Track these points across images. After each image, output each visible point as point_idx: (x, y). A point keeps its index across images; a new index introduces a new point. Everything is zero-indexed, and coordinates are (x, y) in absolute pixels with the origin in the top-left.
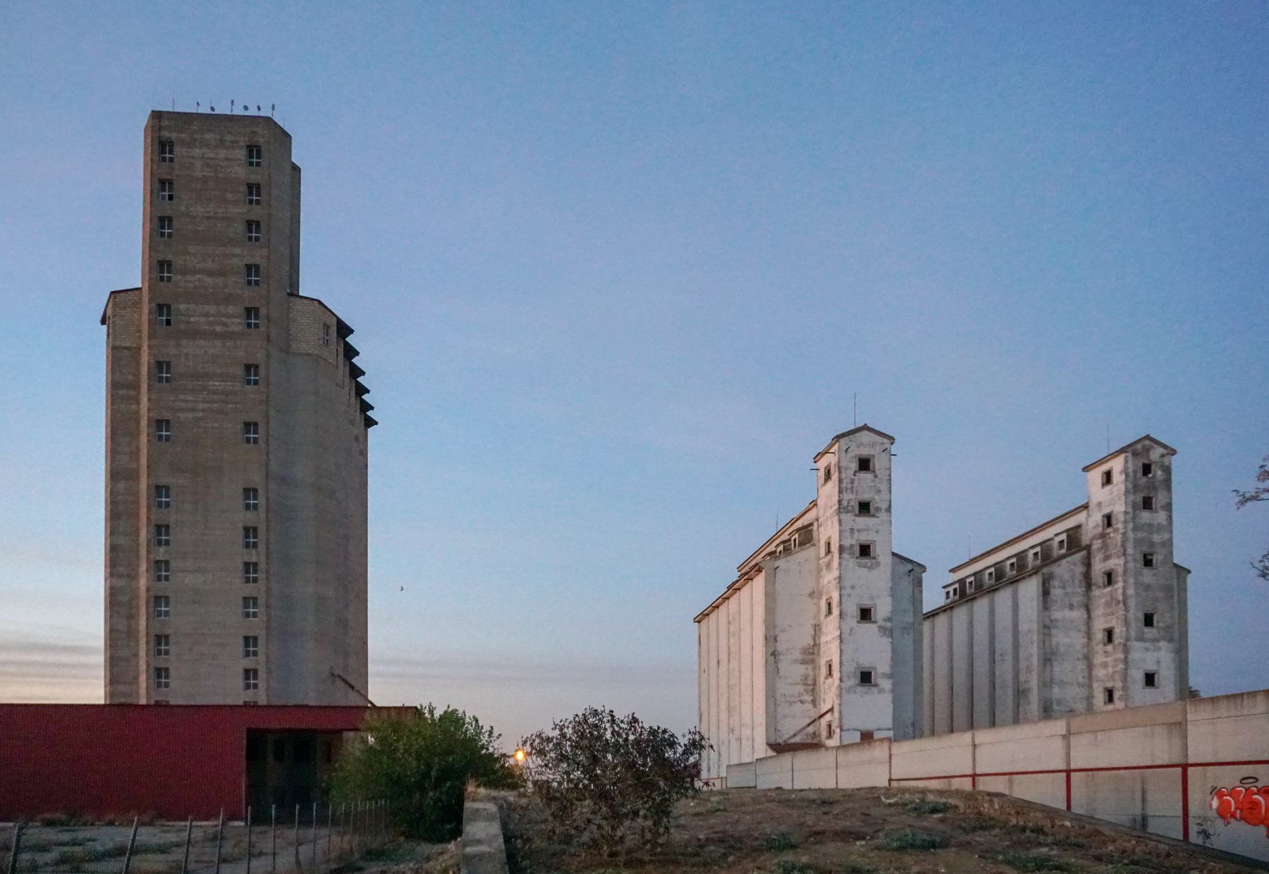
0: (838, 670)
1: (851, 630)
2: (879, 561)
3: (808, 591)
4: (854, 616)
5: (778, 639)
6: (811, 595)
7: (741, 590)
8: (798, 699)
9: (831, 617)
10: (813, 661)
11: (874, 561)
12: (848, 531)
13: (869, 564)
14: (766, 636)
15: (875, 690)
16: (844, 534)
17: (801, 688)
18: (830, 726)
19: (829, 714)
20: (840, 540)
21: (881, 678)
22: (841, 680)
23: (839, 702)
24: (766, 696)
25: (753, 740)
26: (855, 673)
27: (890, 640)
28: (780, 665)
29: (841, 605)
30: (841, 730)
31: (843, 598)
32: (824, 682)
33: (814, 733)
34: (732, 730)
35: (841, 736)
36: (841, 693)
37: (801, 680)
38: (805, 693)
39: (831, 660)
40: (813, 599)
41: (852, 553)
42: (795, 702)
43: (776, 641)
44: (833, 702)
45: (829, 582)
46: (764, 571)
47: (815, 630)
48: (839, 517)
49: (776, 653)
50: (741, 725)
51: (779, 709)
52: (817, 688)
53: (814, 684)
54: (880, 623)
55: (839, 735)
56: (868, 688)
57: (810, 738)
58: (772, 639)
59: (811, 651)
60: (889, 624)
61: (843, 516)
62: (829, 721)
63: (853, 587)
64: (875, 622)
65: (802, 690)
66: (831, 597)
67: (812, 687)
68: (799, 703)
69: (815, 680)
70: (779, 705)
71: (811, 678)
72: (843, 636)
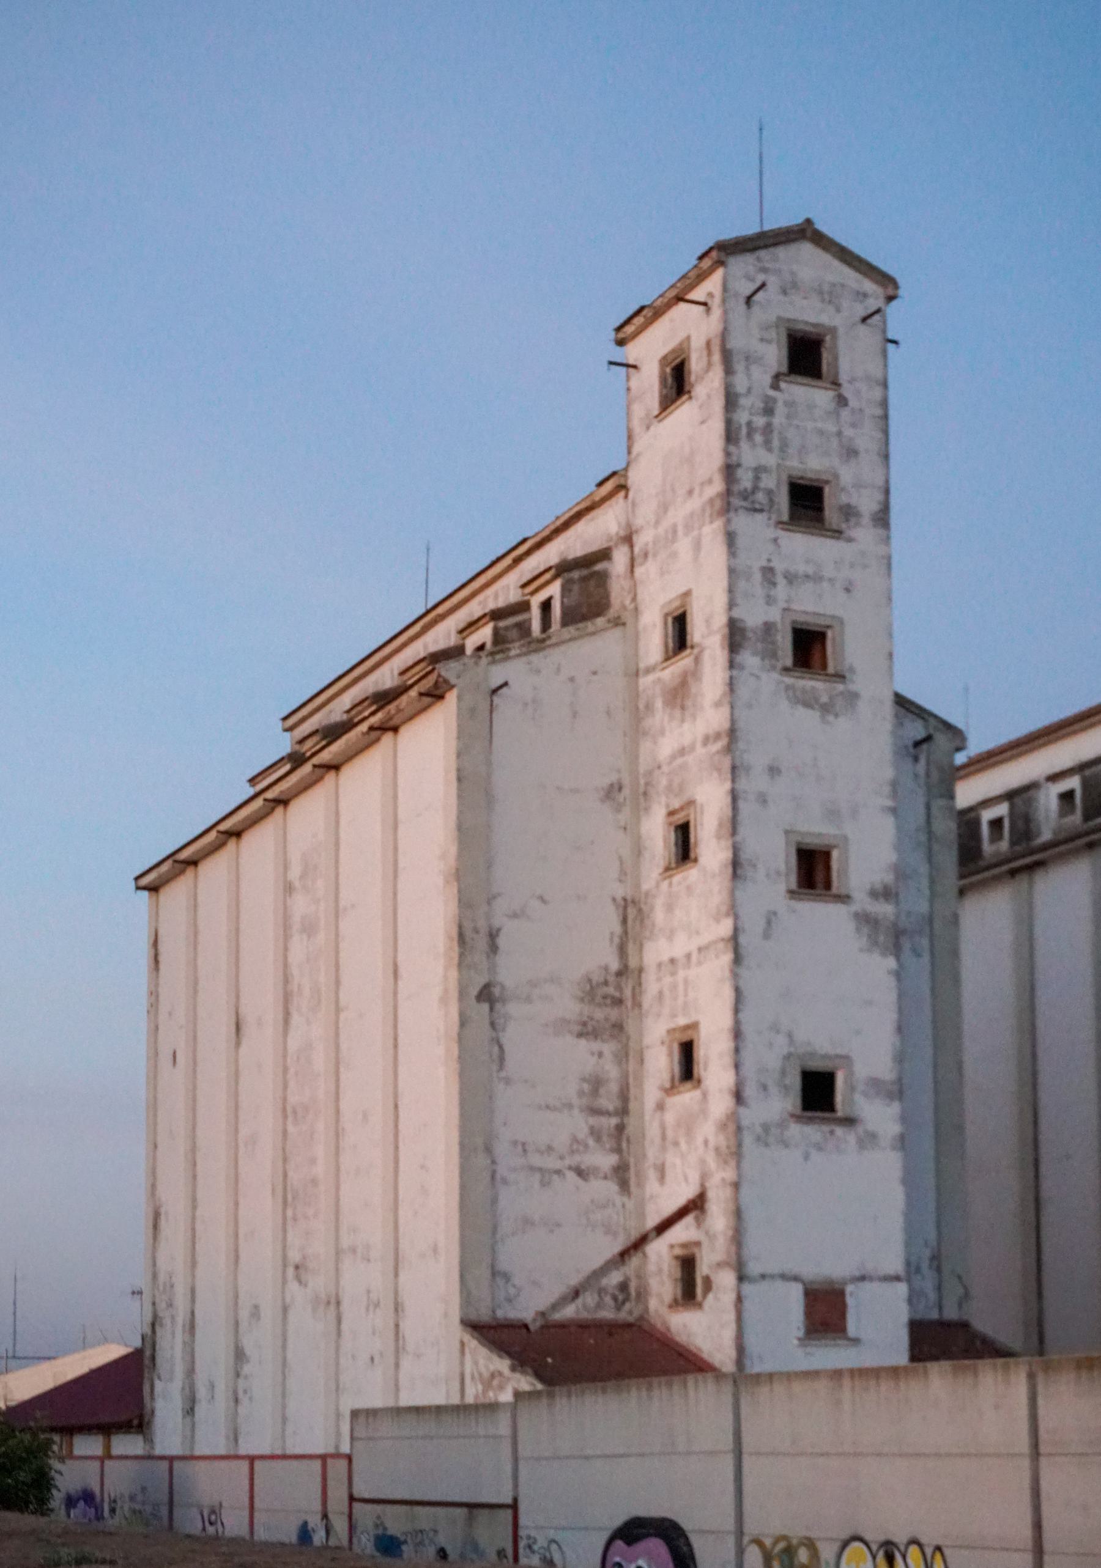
0: (728, 1060)
1: (770, 919)
2: (852, 687)
3: (606, 782)
4: (778, 873)
5: (501, 941)
6: (612, 791)
7: (403, 731)
8: (567, 1162)
9: (692, 874)
10: (618, 1027)
11: (840, 687)
12: (758, 577)
13: (824, 699)
14: (460, 927)
15: (846, 1137)
16: (742, 584)
17: (579, 1124)
18: (687, 1264)
19: (689, 1219)
20: (731, 605)
21: (865, 1094)
22: (739, 1096)
23: (730, 1174)
24: (462, 1146)
25: (398, 1308)
26: (783, 1073)
27: (891, 963)
28: (510, 1037)
29: (734, 832)
30: (741, 1278)
31: (741, 804)
32: (660, 1107)
33: (624, 1287)
34: (297, 1267)
35: (739, 1300)
36: (739, 1145)
37: (581, 1093)
38: (591, 1142)
39: (694, 1026)
40: (618, 809)
41: (770, 654)
42: (558, 1172)
43: (494, 948)
44: (704, 1177)
45: (682, 752)
46: (452, 697)
47: (624, 921)
48: (729, 521)
49: (496, 991)
50: (338, 1252)
51: (505, 1196)
52: (631, 1122)
53: (624, 1111)
54: (862, 901)
55: (729, 1298)
56: (826, 1128)
57: (608, 1299)
58: (482, 943)
59: (611, 990)
60: (885, 910)
61: (743, 522)
62: (684, 1246)
63: (774, 771)
64: (844, 899)
65: (583, 1132)
66: (691, 803)
67: (614, 1121)
68: (571, 1176)
69: (624, 1096)
70: (505, 1181)
71: (614, 1087)
72: (743, 940)
